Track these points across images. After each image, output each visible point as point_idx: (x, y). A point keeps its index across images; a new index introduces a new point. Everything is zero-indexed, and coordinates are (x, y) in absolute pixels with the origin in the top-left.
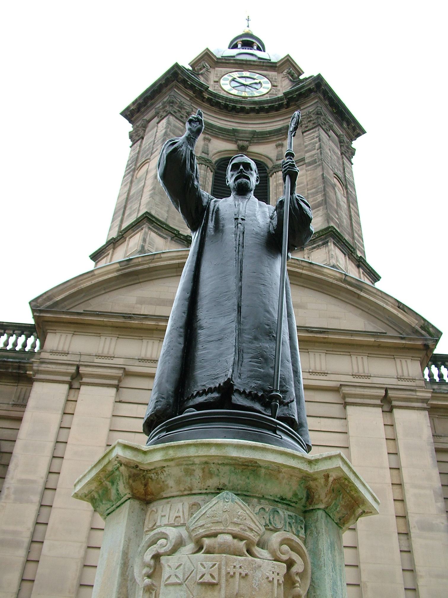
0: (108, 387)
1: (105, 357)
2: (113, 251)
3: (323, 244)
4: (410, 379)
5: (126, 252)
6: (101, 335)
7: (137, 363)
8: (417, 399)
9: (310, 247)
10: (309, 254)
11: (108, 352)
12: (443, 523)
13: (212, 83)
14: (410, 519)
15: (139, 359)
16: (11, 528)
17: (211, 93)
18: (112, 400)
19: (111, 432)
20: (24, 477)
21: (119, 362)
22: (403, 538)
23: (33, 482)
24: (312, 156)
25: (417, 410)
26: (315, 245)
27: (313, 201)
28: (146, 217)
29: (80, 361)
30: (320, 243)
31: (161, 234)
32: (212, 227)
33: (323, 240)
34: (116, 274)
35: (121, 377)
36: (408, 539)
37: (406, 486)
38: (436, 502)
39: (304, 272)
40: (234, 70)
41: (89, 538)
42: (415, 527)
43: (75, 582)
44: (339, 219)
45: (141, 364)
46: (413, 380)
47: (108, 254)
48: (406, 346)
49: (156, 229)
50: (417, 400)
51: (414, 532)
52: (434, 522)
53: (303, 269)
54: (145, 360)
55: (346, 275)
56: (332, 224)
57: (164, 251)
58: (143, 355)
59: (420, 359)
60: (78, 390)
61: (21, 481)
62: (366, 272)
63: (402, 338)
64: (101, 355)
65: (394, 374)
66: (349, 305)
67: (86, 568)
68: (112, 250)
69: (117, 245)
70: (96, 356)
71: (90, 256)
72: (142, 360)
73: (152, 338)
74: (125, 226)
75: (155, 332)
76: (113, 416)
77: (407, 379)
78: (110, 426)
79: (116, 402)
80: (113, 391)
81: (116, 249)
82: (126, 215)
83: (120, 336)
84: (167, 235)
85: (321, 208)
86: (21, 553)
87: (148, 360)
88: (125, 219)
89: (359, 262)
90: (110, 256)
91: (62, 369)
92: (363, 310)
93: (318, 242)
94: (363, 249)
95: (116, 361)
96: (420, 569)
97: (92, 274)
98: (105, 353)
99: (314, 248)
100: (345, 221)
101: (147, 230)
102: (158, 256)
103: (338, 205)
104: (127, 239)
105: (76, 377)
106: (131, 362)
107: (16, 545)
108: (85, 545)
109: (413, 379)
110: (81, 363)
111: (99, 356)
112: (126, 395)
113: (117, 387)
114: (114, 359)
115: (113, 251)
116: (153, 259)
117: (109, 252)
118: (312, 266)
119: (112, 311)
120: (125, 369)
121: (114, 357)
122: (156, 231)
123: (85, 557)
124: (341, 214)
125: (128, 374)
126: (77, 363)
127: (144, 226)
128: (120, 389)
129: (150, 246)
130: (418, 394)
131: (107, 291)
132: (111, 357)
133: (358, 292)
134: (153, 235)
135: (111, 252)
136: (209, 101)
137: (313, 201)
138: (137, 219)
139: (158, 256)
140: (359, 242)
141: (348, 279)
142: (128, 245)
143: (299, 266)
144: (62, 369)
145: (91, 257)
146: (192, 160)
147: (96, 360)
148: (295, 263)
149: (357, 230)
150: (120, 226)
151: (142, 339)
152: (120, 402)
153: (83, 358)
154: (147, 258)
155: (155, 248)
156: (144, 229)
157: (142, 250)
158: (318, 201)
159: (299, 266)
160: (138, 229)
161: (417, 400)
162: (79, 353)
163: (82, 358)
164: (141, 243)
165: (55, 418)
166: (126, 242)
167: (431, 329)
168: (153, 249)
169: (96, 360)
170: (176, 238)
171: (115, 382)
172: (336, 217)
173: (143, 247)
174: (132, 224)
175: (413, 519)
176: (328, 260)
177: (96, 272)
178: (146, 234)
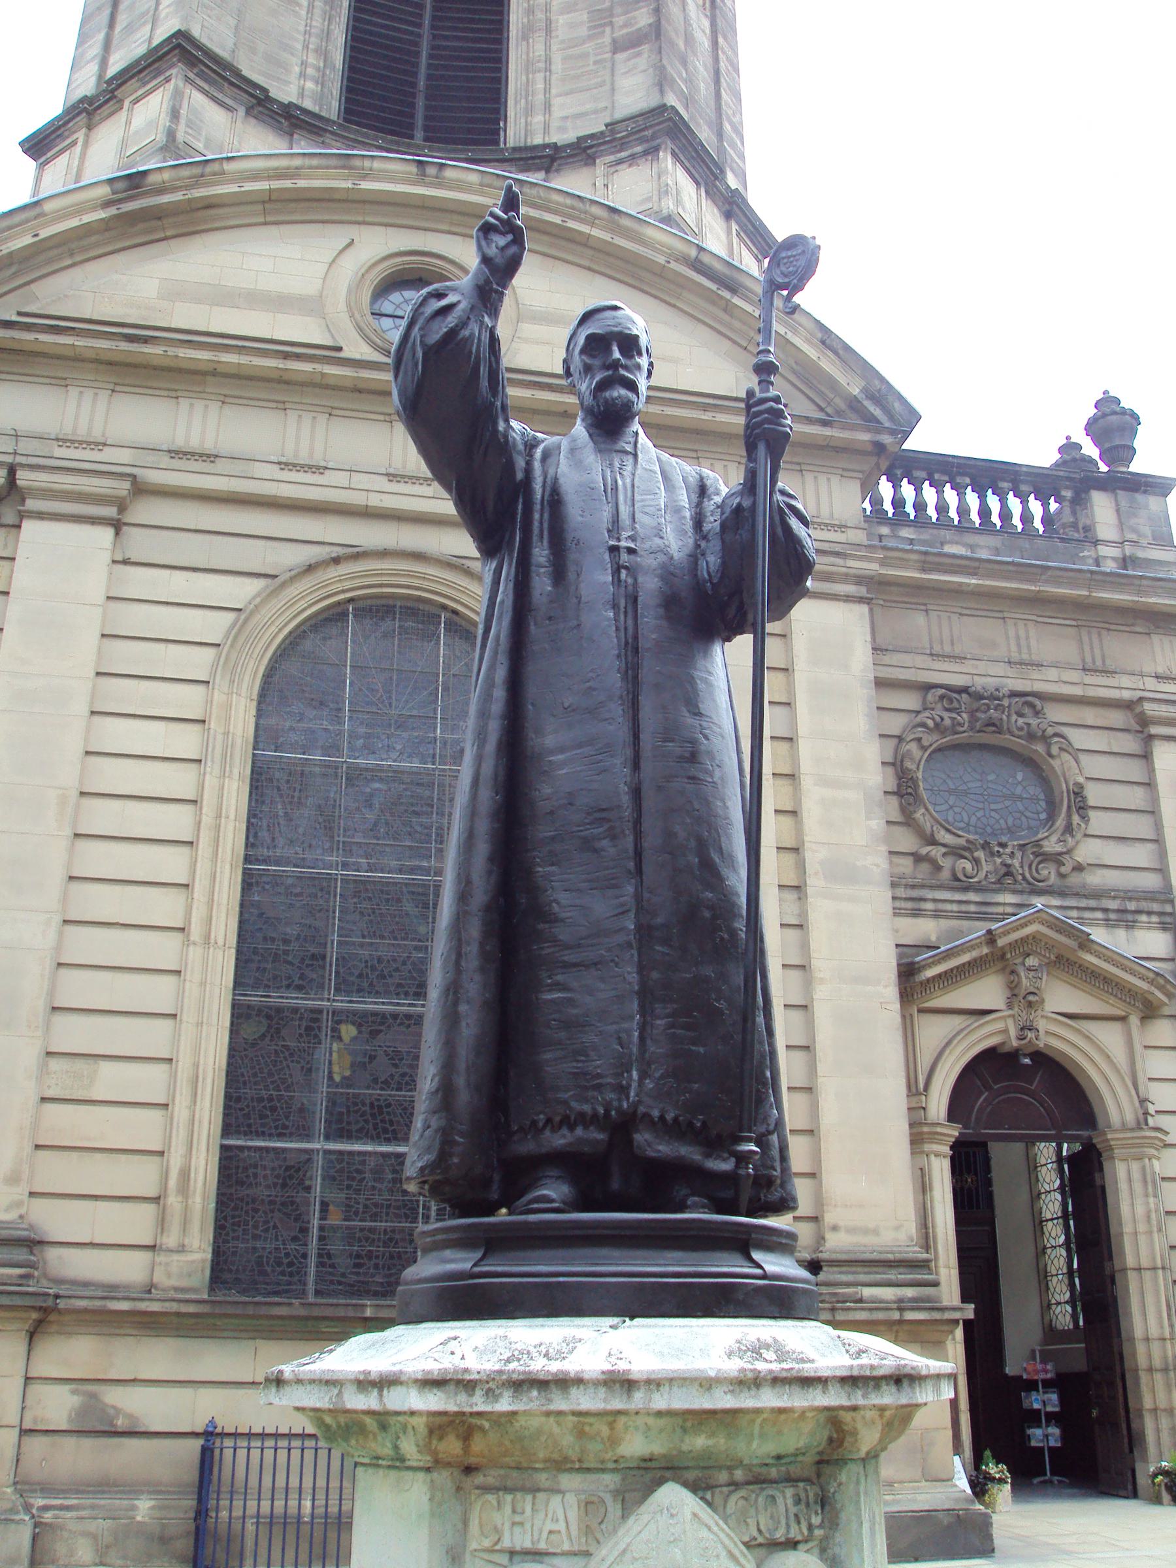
0: (93, 523)
1: (81, 442)
2: (87, 136)
3: (646, 153)
4: (833, 526)
5: (124, 143)
6: (68, 382)
7: (165, 461)
8: (846, 575)
9: (612, 158)
10: (606, 176)
11: (90, 429)
12: (877, 866)
14: (808, 855)
15: (169, 451)
18: (106, 557)
19: (105, 640)
22: (791, 896)
25: (845, 601)
26: (623, 154)
27: (625, 26)
28: (179, 46)
29: (15, 453)
30: (639, 149)
31: (220, 96)
32: (542, 560)
33: (647, 141)
34: (102, 214)
35: (124, 498)
36: (800, 899)
37: (806, 782)
38: (868, 818)
39: (596, 232)
41: (65, 899)
42: (816, 874)
43: (41, 1005)
44: (689, 81)
45: (176, 464)
46: (842, 527)
47: (74, 143)
48: (831, 444)
49: (206, 81)
50: (846, 578)
51: (814, 883)
52: (858, 863)
53: (592, 225)
54: (185, 453)
55: (701, 249)
56: (671, 100)
57: (230, 155)
58: (180, 443)
59: (861, 475)
60: (14, 531)
62: (745, 232)
63: (825, 423)
64: (70, 437)
66: (700, 327)
67: (63, 971)
68: (84, 130)
69: (97, 118)
70: (57, 440)
71: (21, 144)
72: (177, 452)
73: (202, 395)
74: (116, 64)
75: (209, 378)
76: (108, 598)
77: (826, 525)
78: (103, 625)
79: (114, 562)
80: (107, 533)
81: (96, 130)
82: (118, 28)
83: (118, 388)
84: (235, 99)
85: (645, 48)
87: (193, 454)
88: (115, 42)
89: (730, 203)
90: (78, 149)
92: (734, 342)
93: (632, 147)
94: (741, 165)
95: (108, 455)
96: (821, 965)
97: (37, 210)
98: (82, 433)
99: (620, 162)
100: (704, 89)
101: (181, 84)
102: (216, 167)
103: (689, 40)
104: (127, 103)
105: (9, 494)
106: (150, 459)
108: (57, 919)
109: (840, 526)
110: (19, 459)
111: (65, 441)
112: (139, 543)
113: (117, 526)
114: (106, 449)
115: (87, 136)
116: (202, 176)
117: (75, 137)
118: (616, 217)
119: (95, 317)
120: (134, 477)
121: (105, 445)
122: (206, 87)
123: (58, 947)
124: (695, 68)
125: (140, 489)
126: (9, 459)
127: (174, 71)
128: (125, 529)
129: (190, 131)
130: (851, 563)
131: (78, 258)
132: (97, 444)
133: (726, 294)
134: (198, 99)
135: (80, 135)
137: (625, 26)
138: (152, 52)
139: (216, 167)
140: (733, 146)
141: (706, 259)
142: (128, 122)
143: (583, 216)
145: (27, 146)
146: (493, 359)
147: (59, 452)
148: (573, 208)
149: (730, 112)
150: (104, 63)
151: (177, 398)
152: (126, 562)
153: (24, 446)
154: (185, 172)
155: (202, 139)
156: (173, 81)
157: (170, 145)
158: (638, 26)
159: (583, 216)
160: (155, 78)
161: (846, 578)
162: (13, 432)
163: (20, 444)
164: (165, 121)
166: (123, 115)
167: (897, 405)
168: (199, 140)
169: (59, 452)
170: (260, 109)
171: (111, 512)
172: (680, 77)
173: (171, 134)
174: (137, 62)
175: (814, 856)
176: (655, 198)
177: (48, 207)
178: (178, 95)
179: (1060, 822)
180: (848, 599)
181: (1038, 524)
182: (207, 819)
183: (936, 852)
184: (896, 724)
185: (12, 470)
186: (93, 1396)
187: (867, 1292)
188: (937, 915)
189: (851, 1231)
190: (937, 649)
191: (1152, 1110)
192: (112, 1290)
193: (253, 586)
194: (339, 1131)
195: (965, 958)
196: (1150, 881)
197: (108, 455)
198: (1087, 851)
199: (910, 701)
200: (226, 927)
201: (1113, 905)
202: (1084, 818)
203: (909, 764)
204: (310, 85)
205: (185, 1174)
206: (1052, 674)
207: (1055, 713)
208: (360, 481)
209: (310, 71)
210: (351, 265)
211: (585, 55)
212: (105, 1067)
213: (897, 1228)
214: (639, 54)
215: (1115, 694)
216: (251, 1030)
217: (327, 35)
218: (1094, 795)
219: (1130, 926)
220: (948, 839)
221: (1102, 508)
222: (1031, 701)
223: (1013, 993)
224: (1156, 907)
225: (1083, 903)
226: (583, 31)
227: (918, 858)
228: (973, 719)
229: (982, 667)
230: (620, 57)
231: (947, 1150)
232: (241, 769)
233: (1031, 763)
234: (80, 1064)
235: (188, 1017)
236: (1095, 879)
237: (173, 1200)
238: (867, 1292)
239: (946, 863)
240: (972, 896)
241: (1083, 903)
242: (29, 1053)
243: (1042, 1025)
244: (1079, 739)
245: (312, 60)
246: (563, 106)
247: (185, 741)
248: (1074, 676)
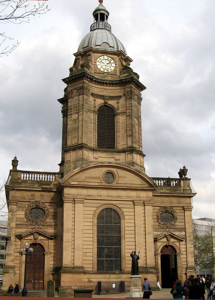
13: (93, 63)
16: (68, 238)
17: (96, 78)
20: (67, 227)
21: (83, 196)
23: (69, 228)
24: (129, 113)
40: (101, 55)
61: (67, 228)
65: (145, 196)
86: (70, 243)
91: (70, 199)
106: (86, 196)
107: (69, 242)
112: (85, 205)
125: (85, 199)
136: (95, 81)
144: (70, 199)
161: (151, 203)
165: (71, 213)
171: (82, 202)
179: (174, 221)
180: (150, 205)
181: (174, 185)
182: (94, 231)
183: (160, 225)
184: (157, 211)
185: (74, 199)
186: (89, 279)
187: (150, 270)
188: (160, 231)
189: (149, 265)
190: (162, 202)
191: (181, 251)
192: (90, 271)
193: (95, 209)
194: (106, 258)
195: (163, 237)
196: (184, 227)
197: (82, 196)
198: (177, 224)
199: (159, 208)
200: (96, 241)
201: (179, 230)
202: (177, 220)
203: (158, 216)
204: (94, 143)
205: (95, 262)
206: (174, 204)
207: (174, 208)
208: (105, 197)
209: (94, 141)
210: (102, 172)
211: (124, 136)
212: (87, 253)
213: (153, 265)
214: (130, 138)
215: (181, 206)
216: (98, 249)
217: (95, 135)
218: (178, 217)
219: (181, 232)
220: (162, 223)
221: (182, 182)
222: (172, 207)
223: (167, 239)
224: (184, 230)
225: (176, 230)
226: (124, 132)
227: (158, 226)
228: (165, 210)
229: (166, 204)
230: (128, 138)
231: (160, 256)
232: (96, 226)
233: (172, 214)
234: (85, 253)
235: (94, 249)
236: (177, 227)
237: (94, 264)
238: (150, 270)
239: (162, 226)
240: (164, 229)
241: (176, 230)
242: (82, 253)
243: (170, 243)
244: (177, 211)
245: (94, 139)
246: (122, 143)
247: (91, 224)
248: (177, 204)
